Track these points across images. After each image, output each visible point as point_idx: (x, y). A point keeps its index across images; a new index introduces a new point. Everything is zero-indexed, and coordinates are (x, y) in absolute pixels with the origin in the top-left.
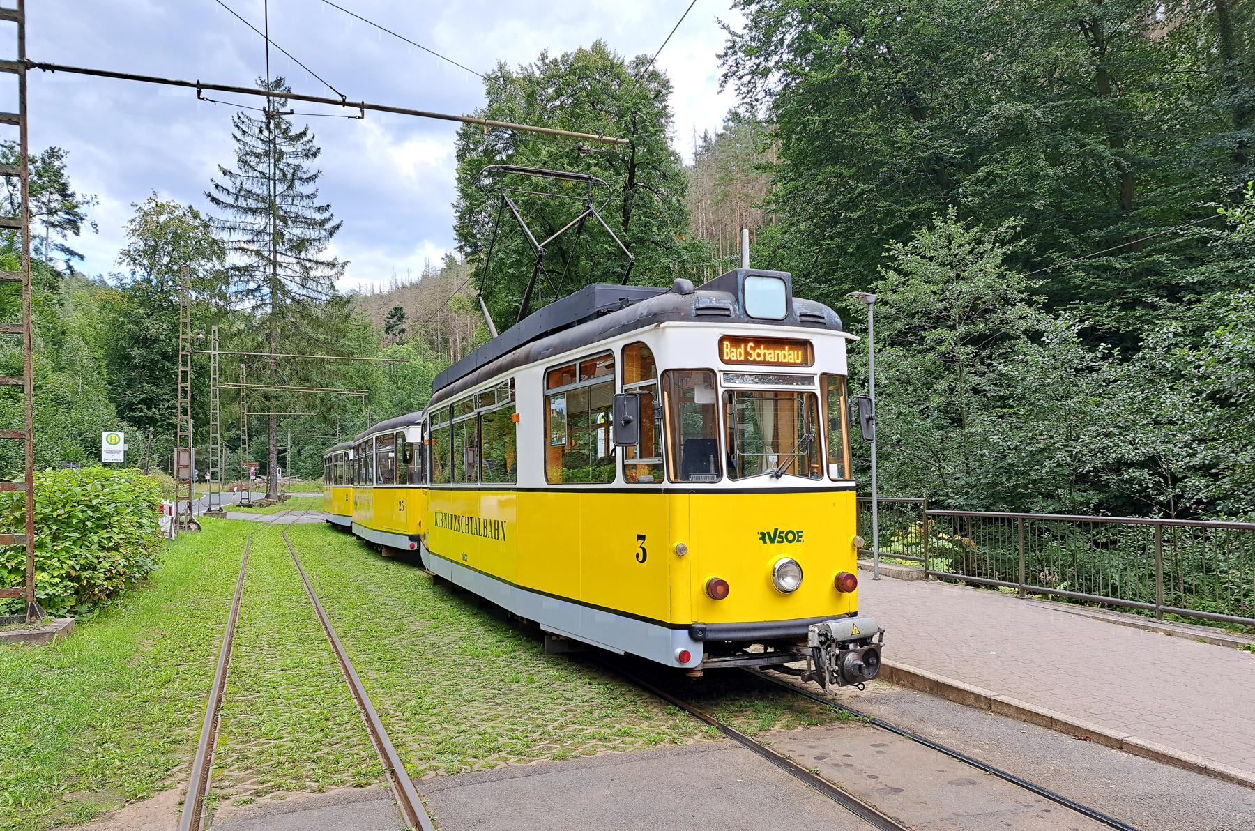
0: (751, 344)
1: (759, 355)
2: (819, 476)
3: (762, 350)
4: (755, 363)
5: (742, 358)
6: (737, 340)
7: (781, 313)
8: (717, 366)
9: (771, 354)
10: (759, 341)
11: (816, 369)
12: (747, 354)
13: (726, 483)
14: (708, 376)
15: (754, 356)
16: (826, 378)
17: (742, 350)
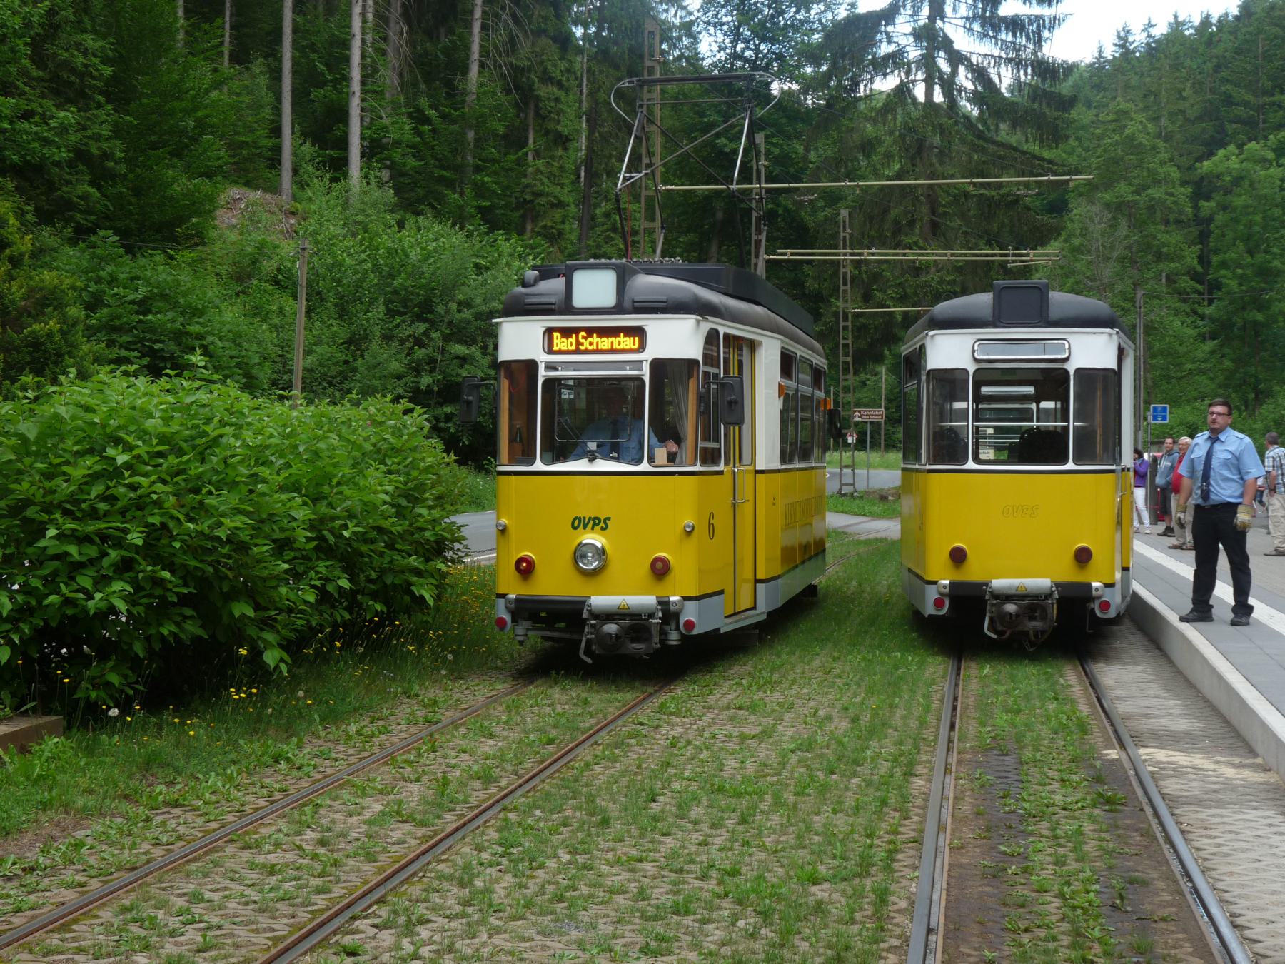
0: (583, 334)
1: (591, 344)
2: (639, 461)
3: (595, 339)
4: (587, 352)
6: (566, 332)
7: (609, 300)
8: (542, 358)
9: (605, 343)
10: (590, 331)
11: (648, 356)
12: (578, 343)
13: (539, 466)
14: (531, 366)
15: (586, 345)
16: (658, 366)
17: (573, 340)
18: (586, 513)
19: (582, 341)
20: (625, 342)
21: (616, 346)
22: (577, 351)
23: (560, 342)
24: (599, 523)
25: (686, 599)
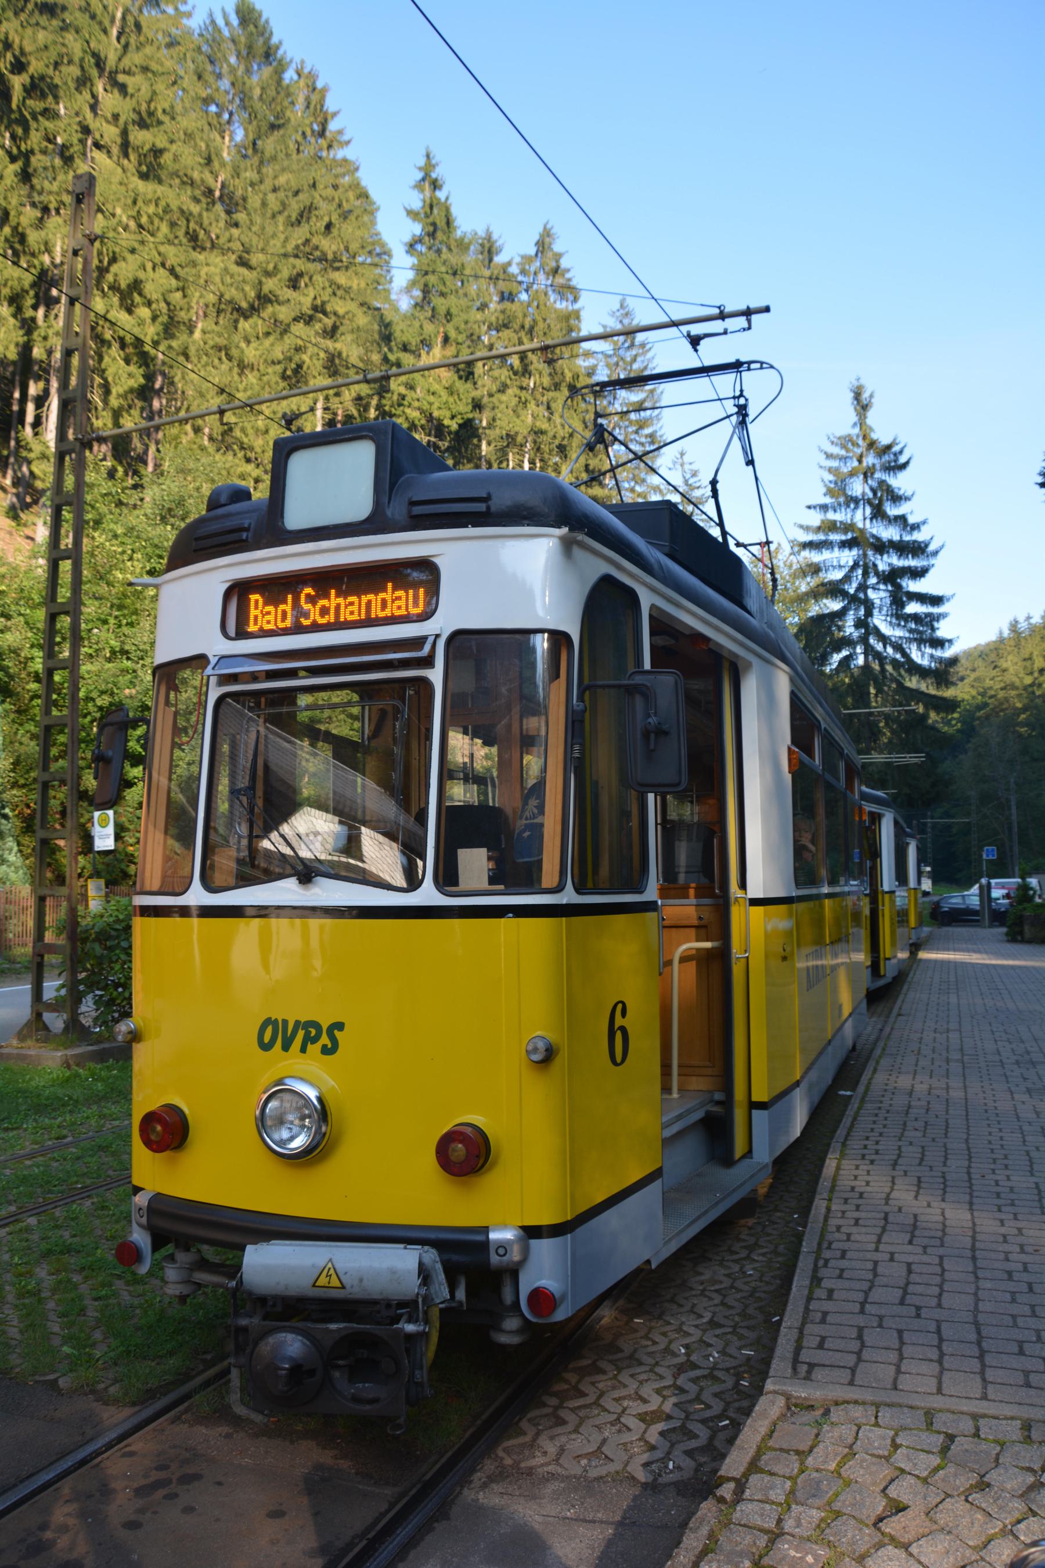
0: (309, 590)
1: (324, 611)
3: (334, 600)
4: (316, 628)
5: (288, 623)
6: (277, 587)
9: (352, 607)
11: (443, 624)
15: (315, 615)
18: (293, 1013)
19: (307, 607)
20: (395, 600)
21: (377, 612)
22: (298, 629)
23: (261, 612)
24: (320, 1036)
25: (532, 1232)
